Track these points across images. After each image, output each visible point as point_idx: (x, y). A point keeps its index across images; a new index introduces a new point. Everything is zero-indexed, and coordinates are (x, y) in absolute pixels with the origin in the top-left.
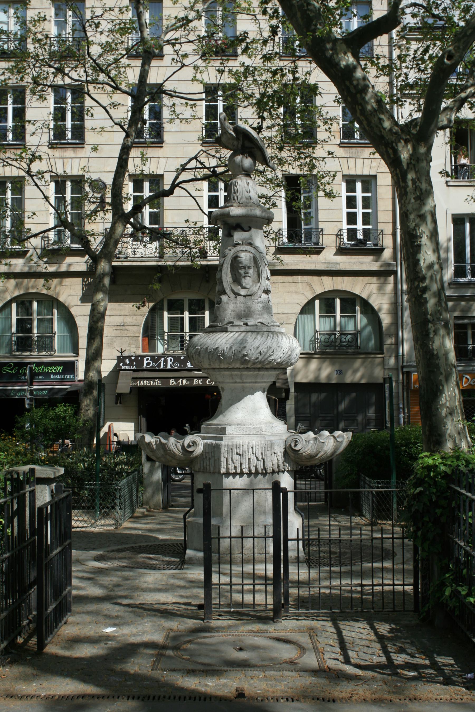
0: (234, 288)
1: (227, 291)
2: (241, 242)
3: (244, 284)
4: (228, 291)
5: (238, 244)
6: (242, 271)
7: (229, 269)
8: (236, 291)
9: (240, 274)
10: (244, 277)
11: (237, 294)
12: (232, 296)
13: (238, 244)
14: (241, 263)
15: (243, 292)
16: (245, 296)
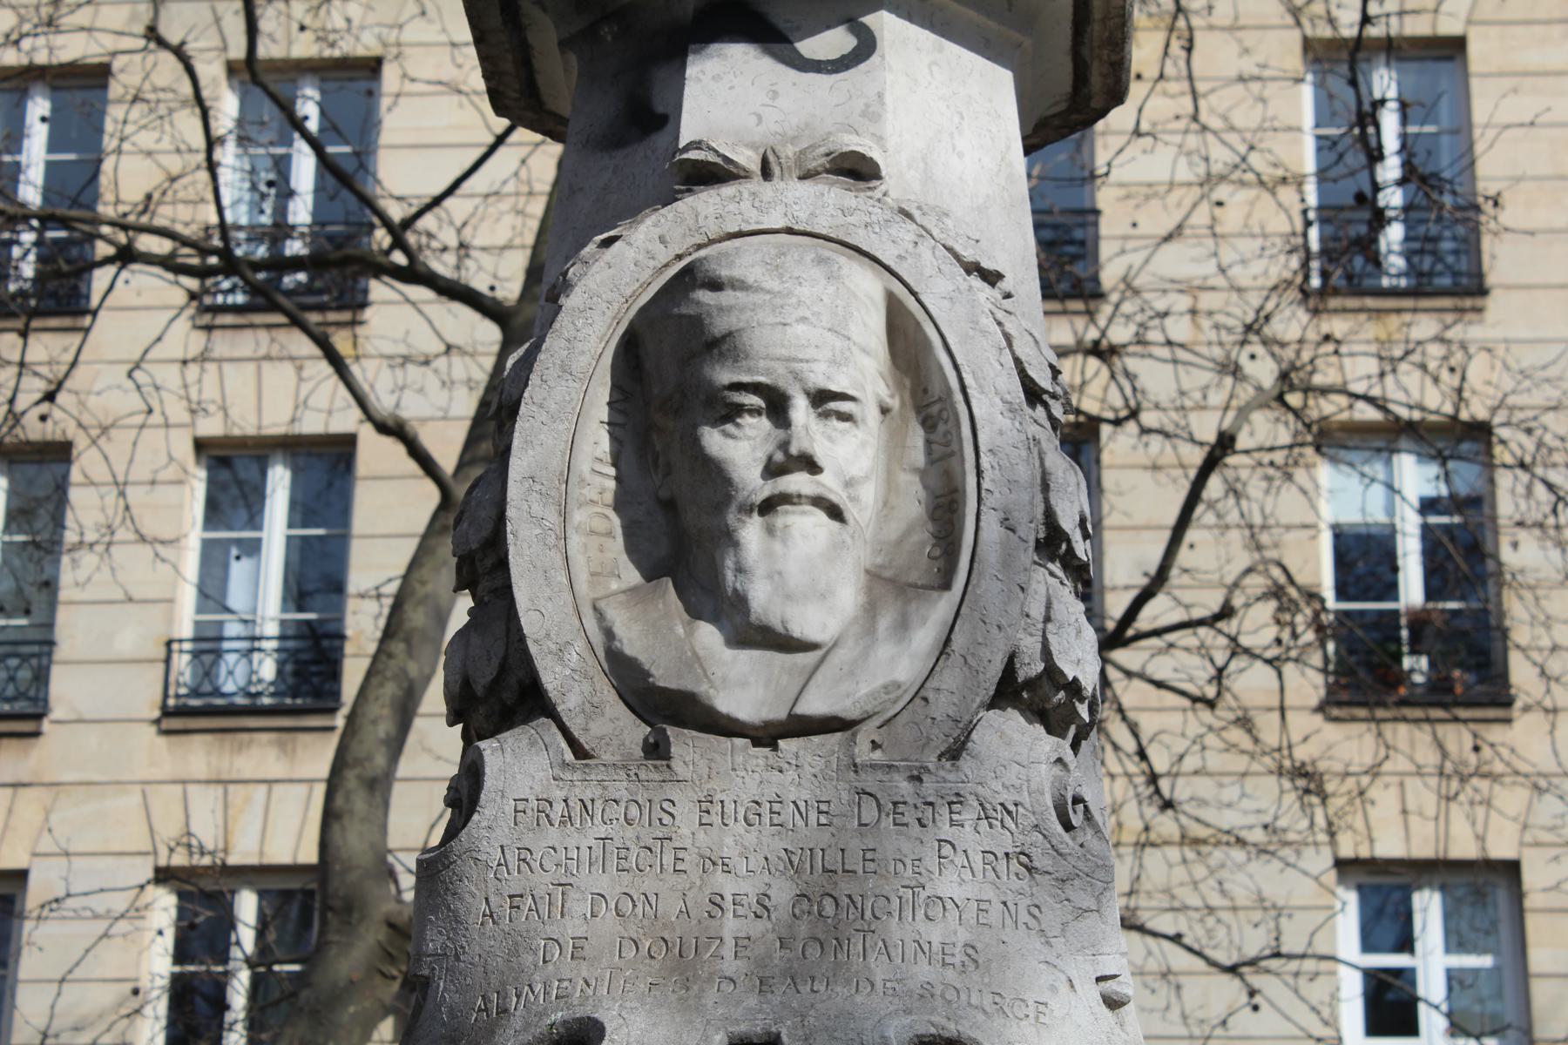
0: (632, 641)
1: (552, 677)
2: (747, 158)
3: (762, 598)
4: (567, 672)
5: (712, 174)
6: (741, 449)
7: (597, 441)
8: (664, 676)
9: (715, 474)
10: (768, 507)
11: (667, 711)
12: (619, 728)
13: (712, 174)
14: (721, 346)
15: (743, 684)
16: (766, 736)
